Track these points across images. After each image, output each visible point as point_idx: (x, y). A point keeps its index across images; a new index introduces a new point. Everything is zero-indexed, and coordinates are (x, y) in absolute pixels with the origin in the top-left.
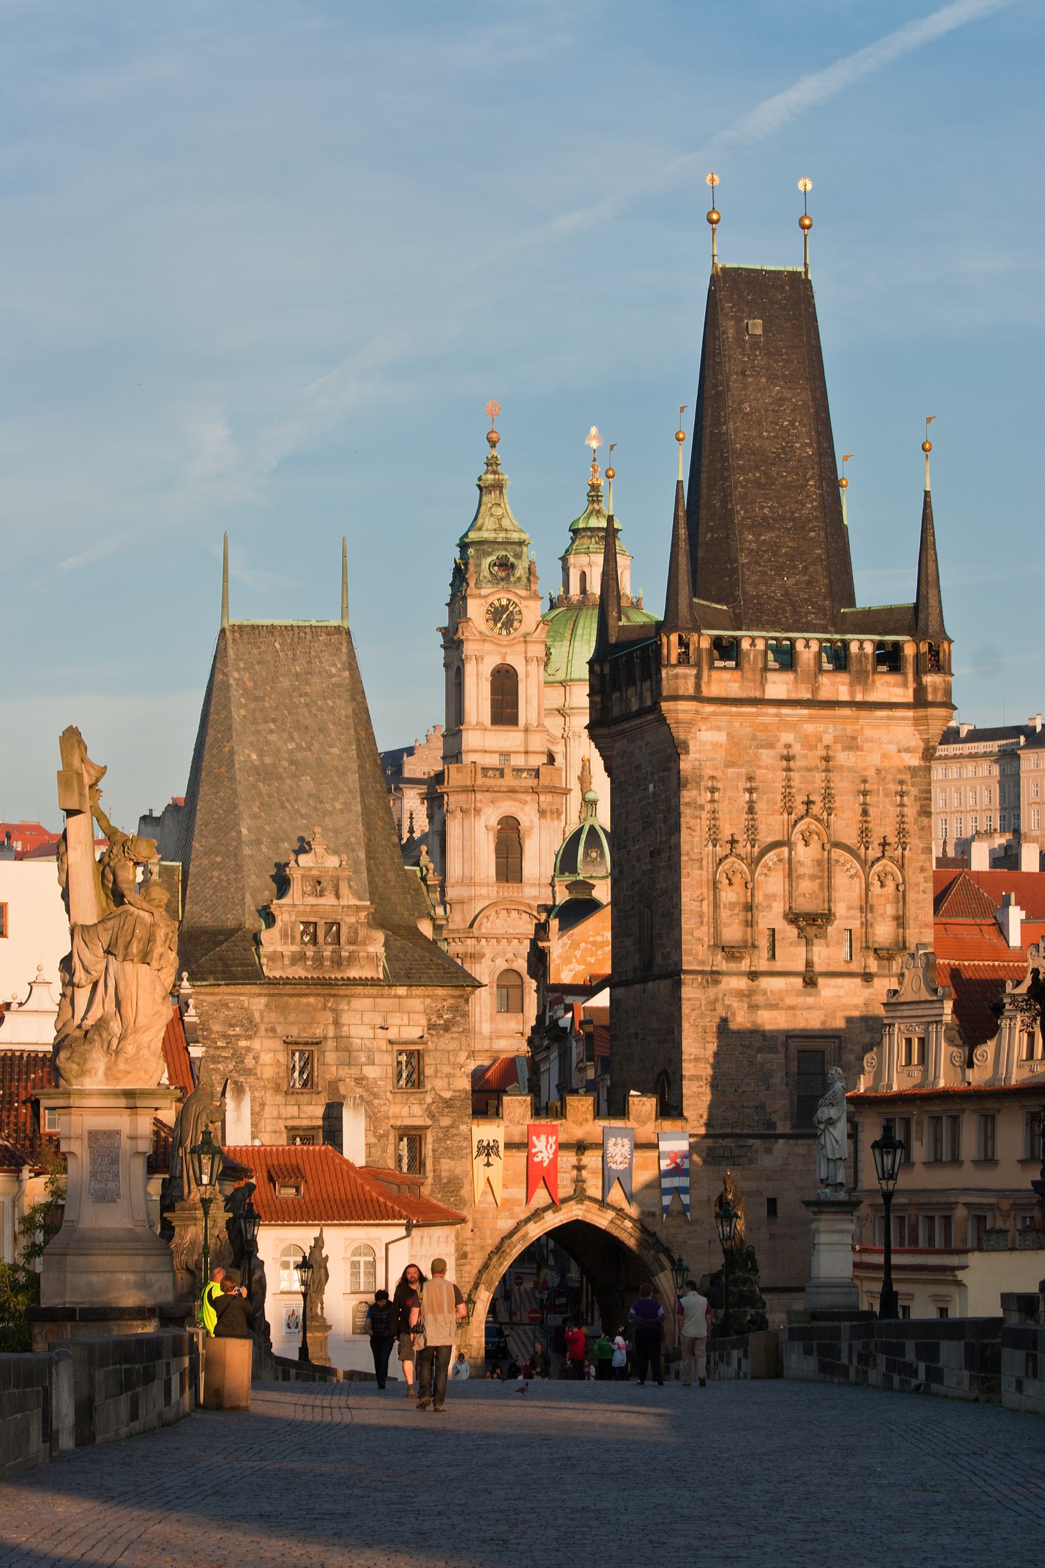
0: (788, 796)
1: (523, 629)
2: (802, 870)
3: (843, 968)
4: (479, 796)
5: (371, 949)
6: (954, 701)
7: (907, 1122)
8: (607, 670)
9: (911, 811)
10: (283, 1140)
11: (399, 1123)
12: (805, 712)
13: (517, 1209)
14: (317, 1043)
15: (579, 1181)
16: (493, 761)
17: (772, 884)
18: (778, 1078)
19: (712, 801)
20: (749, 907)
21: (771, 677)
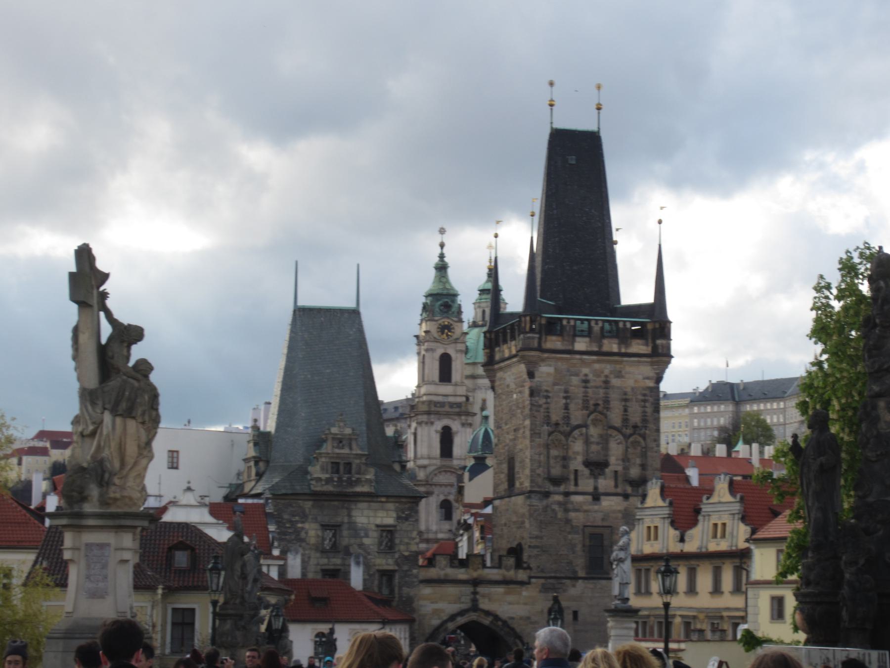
0: (586, 401)
1: (455, 336)
2: (592, 440)
3: (613, 490)
4: (432, 416)
5: (368, 477)
6: (673, 353)
7: (648, 570)
8: (493, 336)
9: (649, 410)
10: (319, 577)
11: (381, 568)
12: (594, 357)
14: (339, 526)
15: (475, 601)
16: (440, 399)
17: (578, 446)
18: (579, 548)
19: (547, 403)
20: (565, 459)
21: (578, 339)
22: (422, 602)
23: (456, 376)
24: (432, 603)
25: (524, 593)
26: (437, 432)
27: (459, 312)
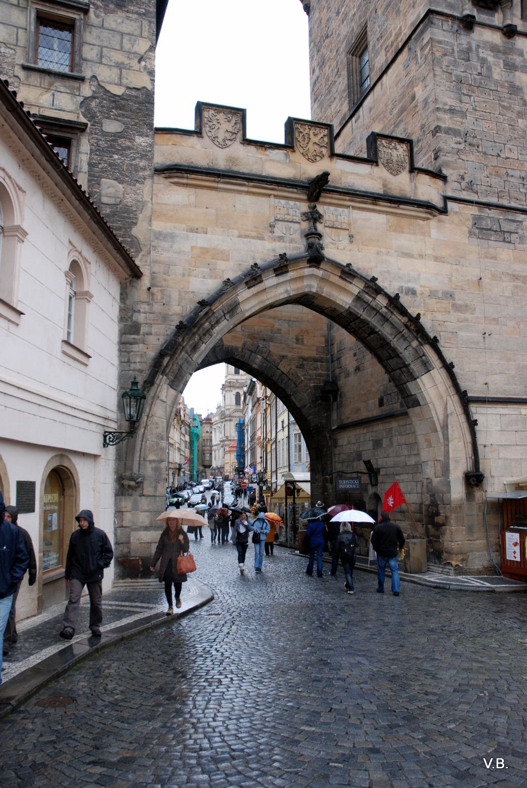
13: (221, 265)
15: (313, 237)
22: (158, 226)
24: (192, 230)
25: (434, 233)
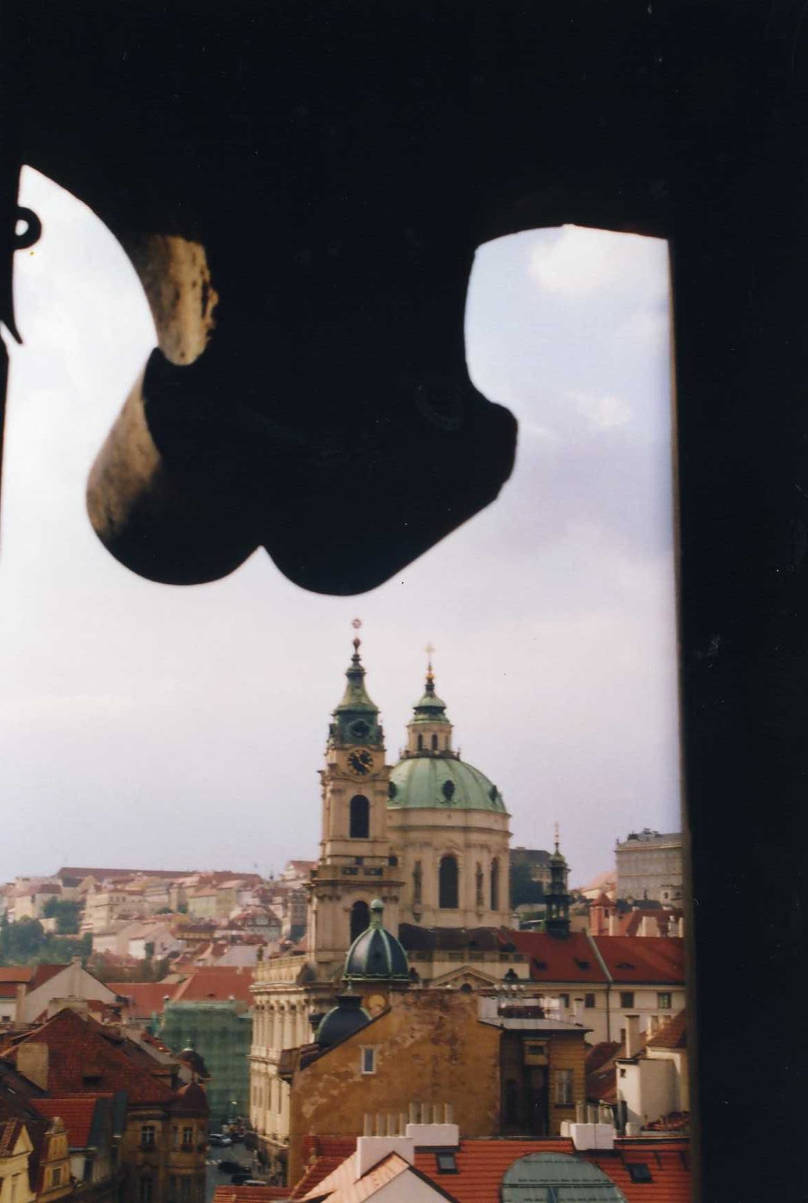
1: (373, 771)
23: (375, 829)
26: (346, 910)
27: (380, 736)
